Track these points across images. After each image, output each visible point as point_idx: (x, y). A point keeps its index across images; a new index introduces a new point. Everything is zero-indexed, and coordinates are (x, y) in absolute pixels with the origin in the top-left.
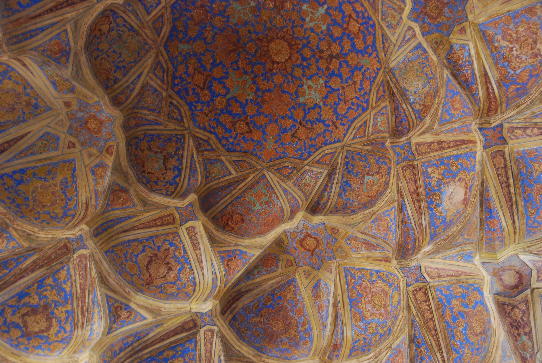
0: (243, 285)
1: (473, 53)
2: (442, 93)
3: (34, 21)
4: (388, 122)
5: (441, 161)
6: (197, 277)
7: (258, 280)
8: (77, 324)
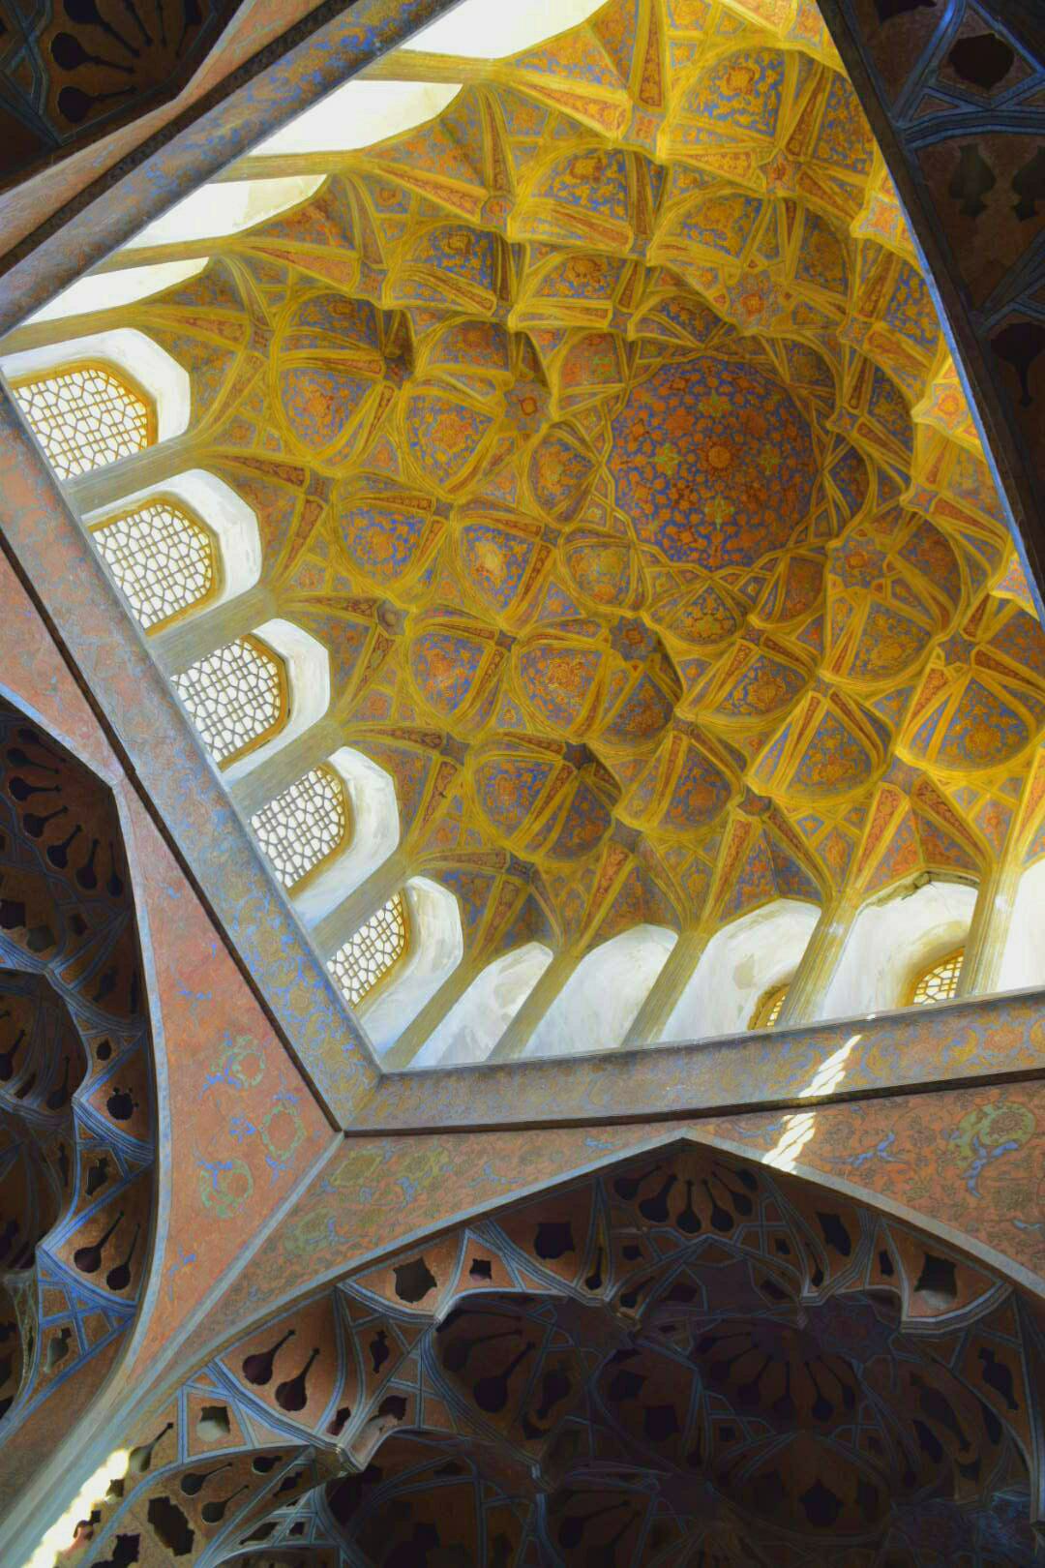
5: (525, 561)
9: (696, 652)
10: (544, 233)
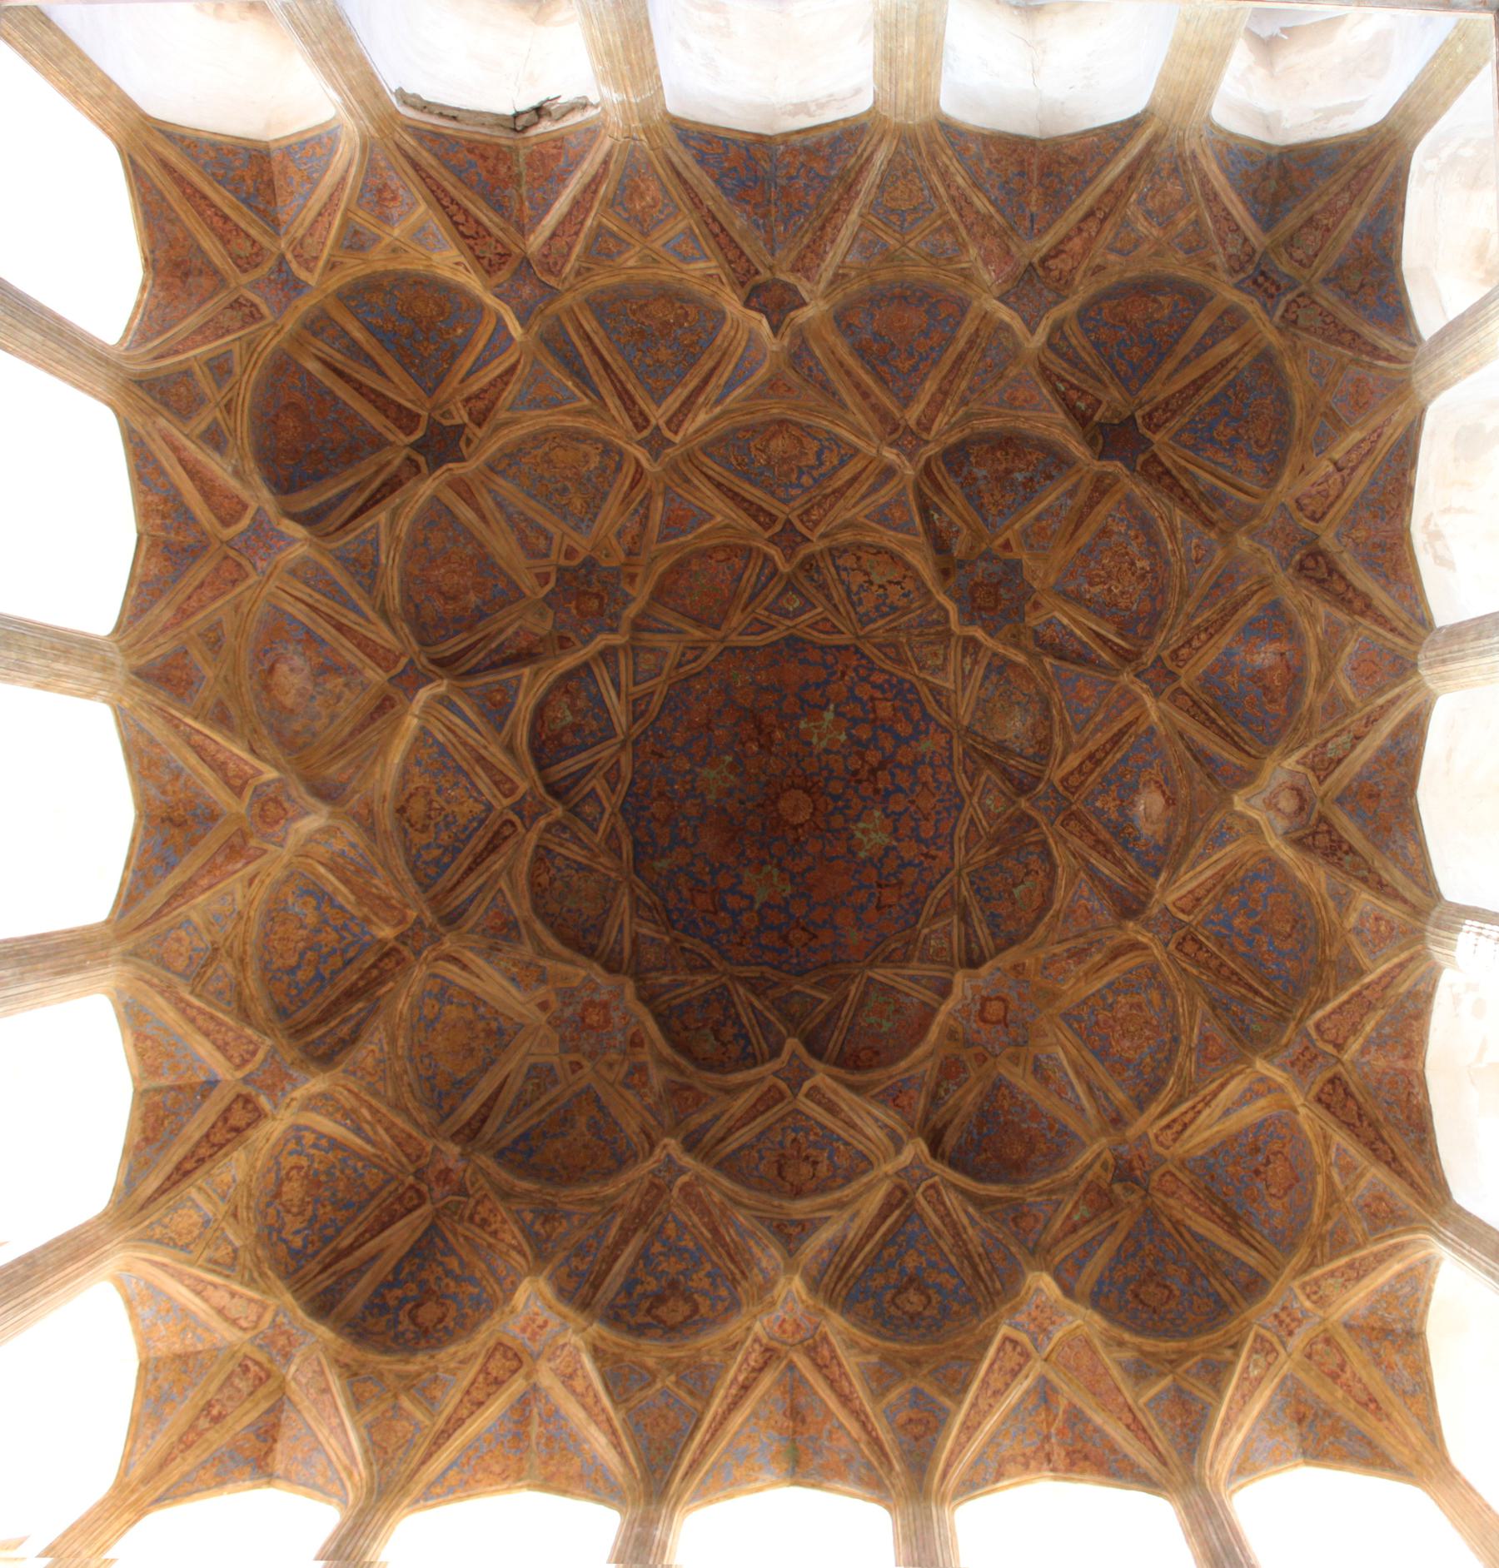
0: (934, 1118)
1: (1065, 621)
2: (1056, 696)
3: (454, 894)
4: (1004, 794)
6: (861, 1147)
7: (951, 1102)
8: (734, 1280)
10: (769, 1255)
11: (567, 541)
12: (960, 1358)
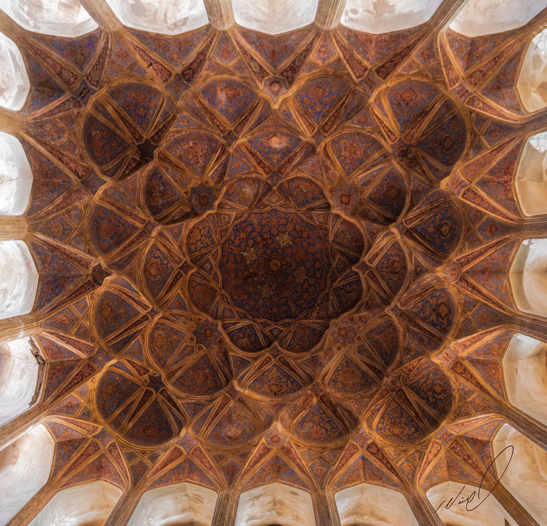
0: (381, 221)
5: (267, 158)
9: (185, 233)
11: (188, 340)
12: (468, 213)
